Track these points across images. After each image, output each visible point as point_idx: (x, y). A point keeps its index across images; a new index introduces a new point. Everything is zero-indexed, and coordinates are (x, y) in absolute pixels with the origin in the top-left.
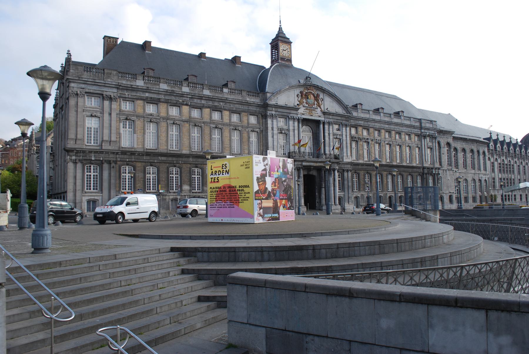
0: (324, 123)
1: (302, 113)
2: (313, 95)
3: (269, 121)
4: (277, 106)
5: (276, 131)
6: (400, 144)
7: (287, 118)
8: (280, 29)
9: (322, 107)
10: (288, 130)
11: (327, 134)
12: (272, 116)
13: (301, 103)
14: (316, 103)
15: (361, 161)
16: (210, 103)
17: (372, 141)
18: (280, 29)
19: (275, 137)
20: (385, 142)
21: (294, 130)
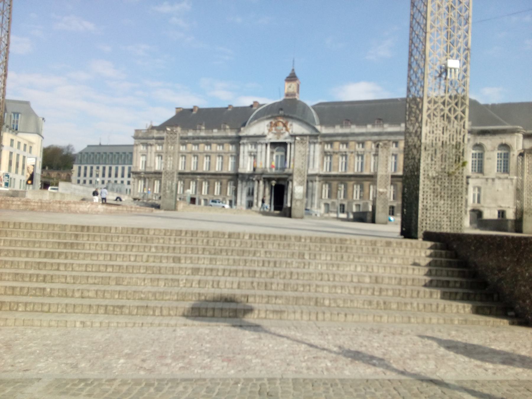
0: (291, 144)
1: (271, 137)
2: (282, 122)
3: (242, 148)
4: (248, 137)
5: (246, 154)
6: (394, 153)
7: (255, 144)
8: (293, 70)
9: (290, 131)
10: (257, 152)
11: (292, 152)
12: (244, 144)
13: (270, 131)
14: (284, 129)
15: (334, 173)
16: (204, 141)
17: (352, 153)
18: (293, 70)
19: (245, 158)
20: (370, 152)
21: (261, 152)
